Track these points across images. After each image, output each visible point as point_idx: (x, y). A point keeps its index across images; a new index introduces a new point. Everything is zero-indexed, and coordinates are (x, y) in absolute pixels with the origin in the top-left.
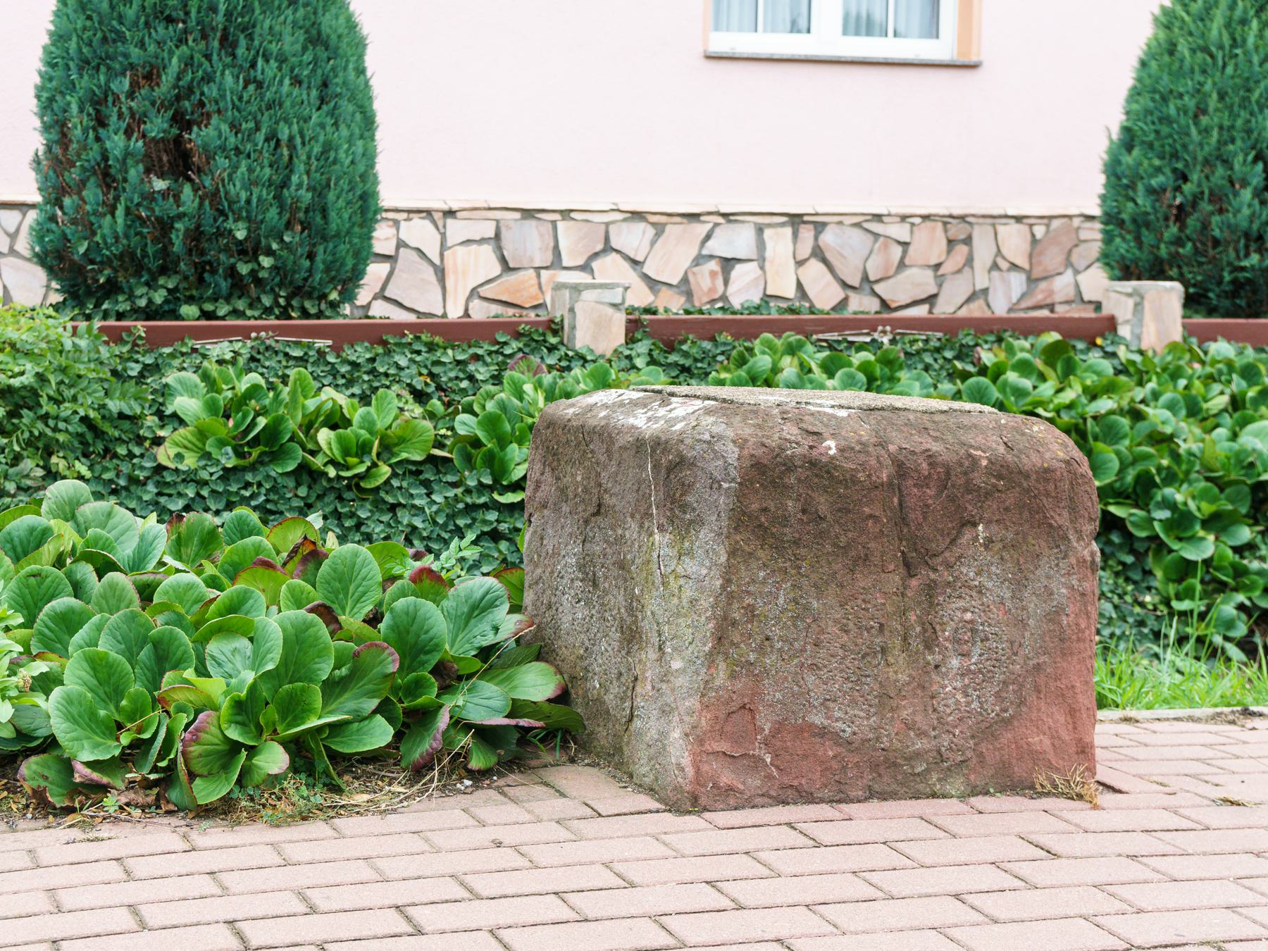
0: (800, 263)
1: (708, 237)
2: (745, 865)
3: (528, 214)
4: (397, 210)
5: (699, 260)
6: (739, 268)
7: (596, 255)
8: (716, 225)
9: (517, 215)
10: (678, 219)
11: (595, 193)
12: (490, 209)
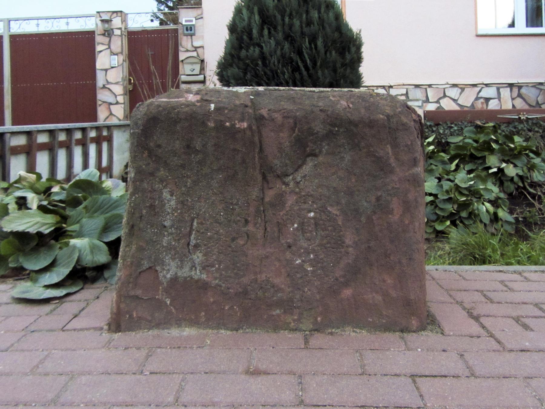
0: (513, 99)
1: (480, 91)
2: (516, 277)
3: (417, 86)
4: (373, 86)
5: (477, 99)
6: (491, 101)
7: (440, 98)
8: (483, 88)
9: (413, 87)
10: (469, 86)
11: (439, 80)
12: (404, 85)
